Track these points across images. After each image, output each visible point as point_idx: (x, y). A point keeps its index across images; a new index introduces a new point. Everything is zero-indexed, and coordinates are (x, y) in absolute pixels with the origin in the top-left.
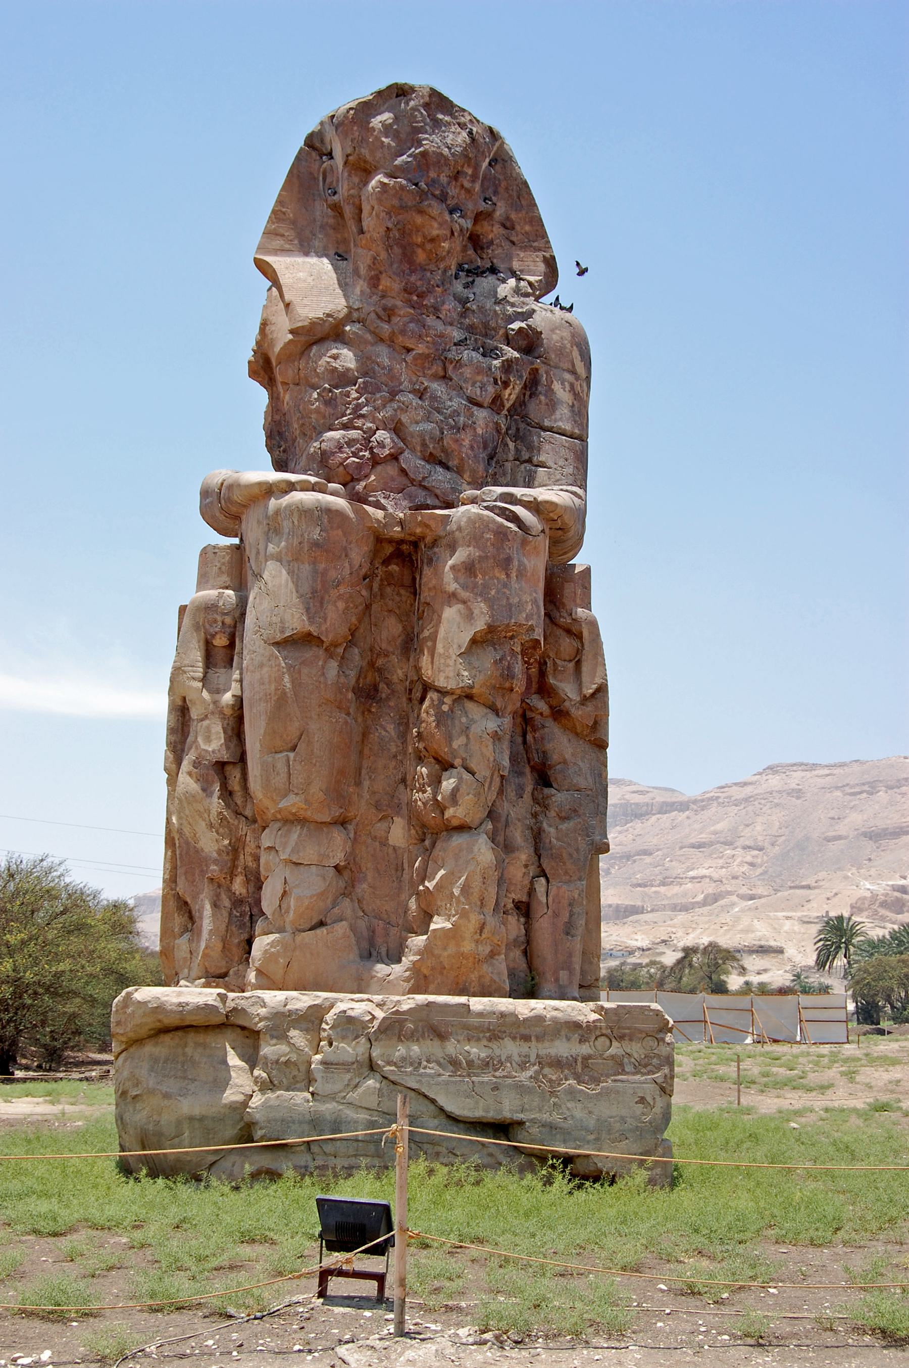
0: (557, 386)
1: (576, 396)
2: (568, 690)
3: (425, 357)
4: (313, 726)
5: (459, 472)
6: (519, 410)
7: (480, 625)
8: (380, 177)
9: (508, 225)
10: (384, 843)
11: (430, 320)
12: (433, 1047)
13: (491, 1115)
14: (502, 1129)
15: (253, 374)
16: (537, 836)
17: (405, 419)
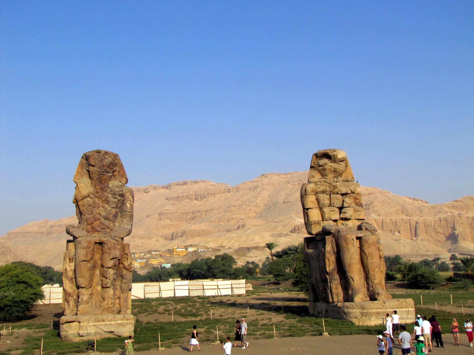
0: (127, 204)
1: (131, 205)
2: (126, 264)
3: (103, 201)
4: (86, 274)
5: (110, 221)
6: (121, 208)
7: (111, 258)
8: (95, 168)
9: (119, 172)
10: (97, 290)
11: (105, 193)
12: (102, 323)
13: (110, 331)
14: (112, 332)
15: (74, 202)
16: (121, 287)
17: (101, 212)
